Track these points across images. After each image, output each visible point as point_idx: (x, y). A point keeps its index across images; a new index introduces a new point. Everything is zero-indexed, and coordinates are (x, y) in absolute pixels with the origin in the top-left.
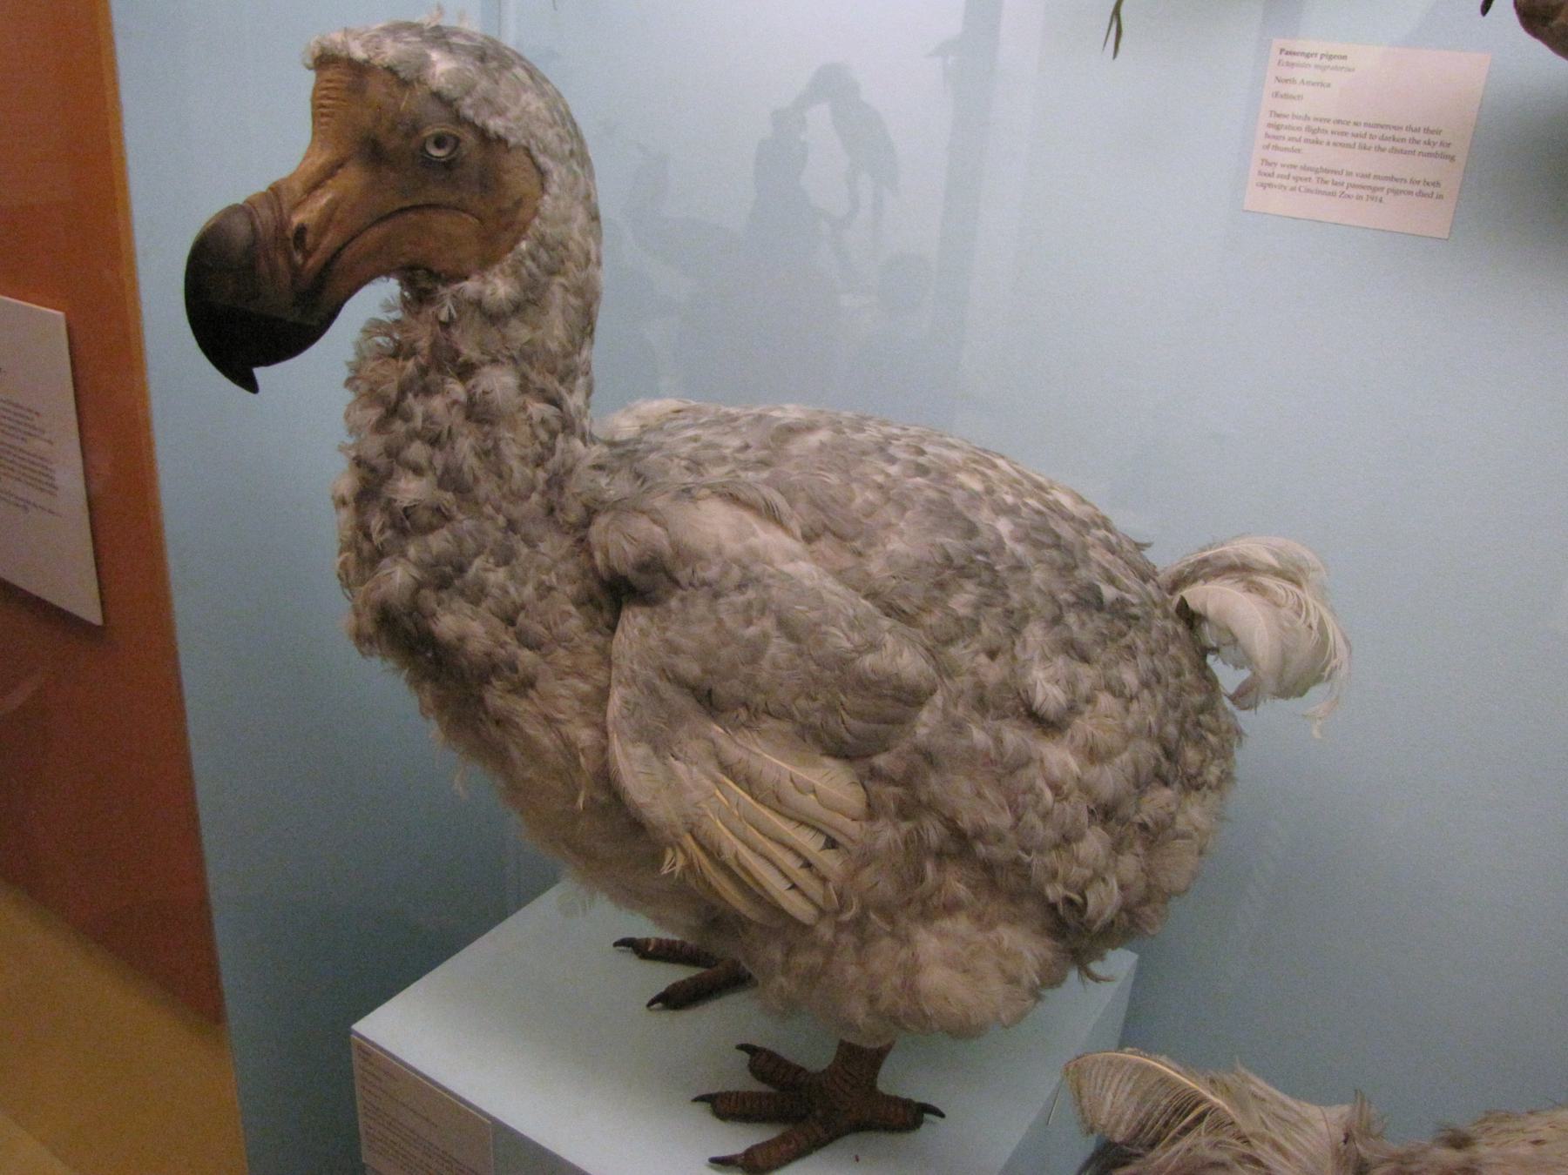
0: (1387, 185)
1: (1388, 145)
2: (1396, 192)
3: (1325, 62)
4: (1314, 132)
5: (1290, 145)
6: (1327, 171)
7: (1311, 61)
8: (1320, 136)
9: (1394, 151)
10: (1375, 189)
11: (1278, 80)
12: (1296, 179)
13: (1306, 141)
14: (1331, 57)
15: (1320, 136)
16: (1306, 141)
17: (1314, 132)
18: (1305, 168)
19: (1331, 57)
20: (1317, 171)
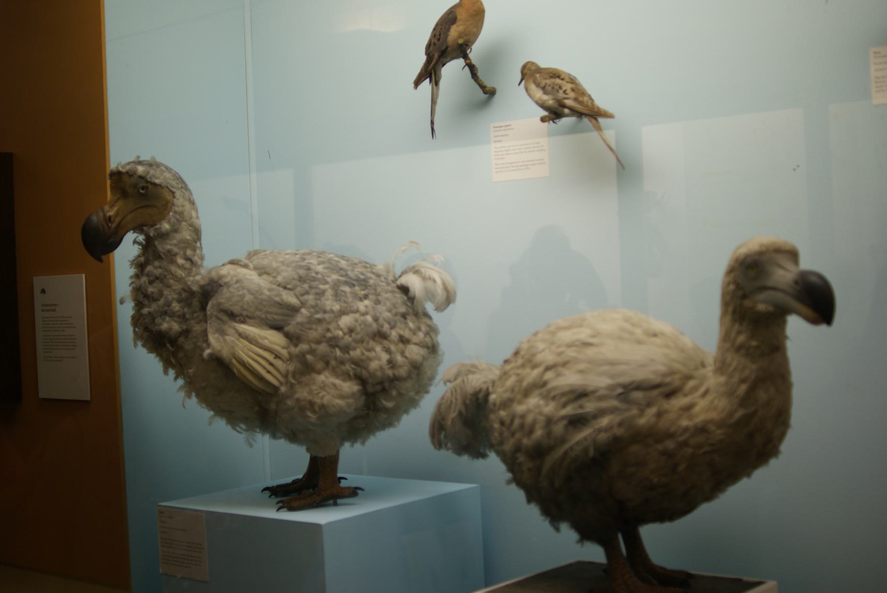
0: (530, 163)
1: (527, 150)
2: (533, 165)
3: (506, 128)
4: (507, 151)
5: (501, 157)
6: (513, 163)
7: (502, 128)
8: (509, 152)
9: (529, 152)
10: (527, 165)
11: (495, 136)
12: (506, 167)
13: (506, 154)
14: (507, 126)
15: (509, 152)
16: (506, 154)
17: (507, 151)
18: (507, 163)
19: (507, 126)
20: (510, 163)
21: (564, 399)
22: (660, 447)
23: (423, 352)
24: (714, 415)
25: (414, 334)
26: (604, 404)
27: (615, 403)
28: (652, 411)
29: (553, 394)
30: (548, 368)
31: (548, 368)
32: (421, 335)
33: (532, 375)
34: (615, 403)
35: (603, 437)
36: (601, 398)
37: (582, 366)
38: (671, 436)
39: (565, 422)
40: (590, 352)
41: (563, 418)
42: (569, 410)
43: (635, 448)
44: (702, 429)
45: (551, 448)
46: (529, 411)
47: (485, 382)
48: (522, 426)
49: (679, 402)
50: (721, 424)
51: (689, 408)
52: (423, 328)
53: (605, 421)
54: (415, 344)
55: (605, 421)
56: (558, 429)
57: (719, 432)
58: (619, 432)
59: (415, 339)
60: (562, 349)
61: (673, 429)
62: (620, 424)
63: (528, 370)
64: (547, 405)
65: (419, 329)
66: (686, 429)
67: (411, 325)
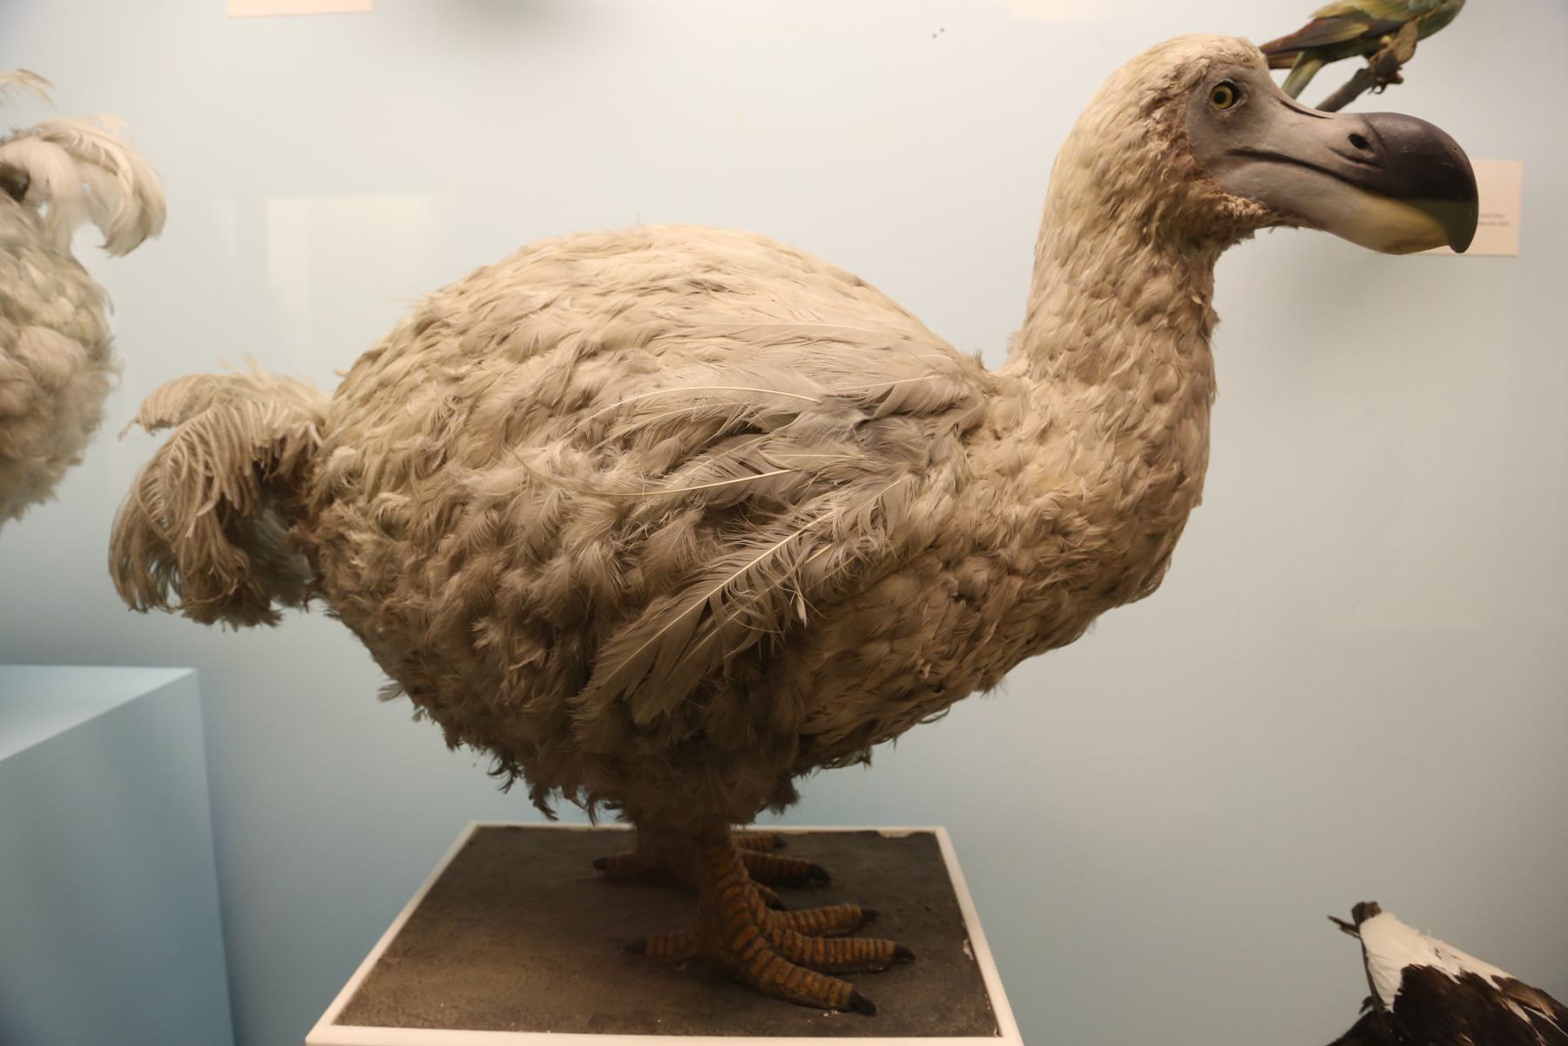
21: (671, 443)
22: (953, 579)
23: (75, 350)
24: (1080, 487)
25: (46, 300)
26: (821, 457)
27: (853, 453)
28: (941, 477)
29: (619, 430)
30: (587, 354)
31: (587, 354)
32: (65, 306)
33: (532, 375)
34: (853, 453)
35: (829, 559)
36: (805, 440)
37: (712, 346)
38: (981, 547)
39: (693, 515)
40: (721, 308)
41: (682, 504)
42: (699, 474)
43: (898, 587)
44: (1052, 527)
45: (633, 602)
46: (534, 484)
47: (297, 418)
48: (501, 535)
49: (988, 454)
50: (1097, 510)
51: (1015, 470)
52: (71, 290)
53: (834, 509)
54: (50, 326)
55: (834, 509)
56: (675, 536)
57: (1093, 530)
58: (877, 541)
59: (47, 313)
60: (615, 300)
61: (985, 529)
62: (878, 516)
63: (497, 363)
64: (603, 465)
65: (61, 291)
66: (1016, 527)
67: (35, 274)
